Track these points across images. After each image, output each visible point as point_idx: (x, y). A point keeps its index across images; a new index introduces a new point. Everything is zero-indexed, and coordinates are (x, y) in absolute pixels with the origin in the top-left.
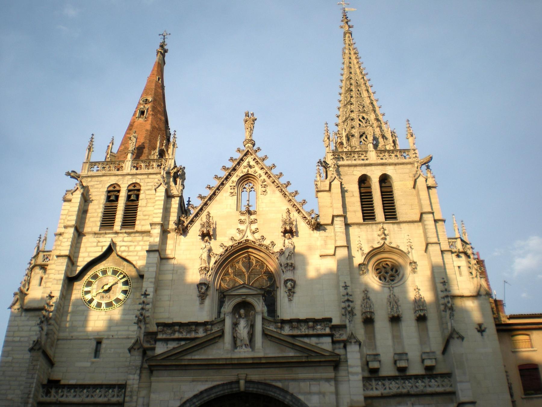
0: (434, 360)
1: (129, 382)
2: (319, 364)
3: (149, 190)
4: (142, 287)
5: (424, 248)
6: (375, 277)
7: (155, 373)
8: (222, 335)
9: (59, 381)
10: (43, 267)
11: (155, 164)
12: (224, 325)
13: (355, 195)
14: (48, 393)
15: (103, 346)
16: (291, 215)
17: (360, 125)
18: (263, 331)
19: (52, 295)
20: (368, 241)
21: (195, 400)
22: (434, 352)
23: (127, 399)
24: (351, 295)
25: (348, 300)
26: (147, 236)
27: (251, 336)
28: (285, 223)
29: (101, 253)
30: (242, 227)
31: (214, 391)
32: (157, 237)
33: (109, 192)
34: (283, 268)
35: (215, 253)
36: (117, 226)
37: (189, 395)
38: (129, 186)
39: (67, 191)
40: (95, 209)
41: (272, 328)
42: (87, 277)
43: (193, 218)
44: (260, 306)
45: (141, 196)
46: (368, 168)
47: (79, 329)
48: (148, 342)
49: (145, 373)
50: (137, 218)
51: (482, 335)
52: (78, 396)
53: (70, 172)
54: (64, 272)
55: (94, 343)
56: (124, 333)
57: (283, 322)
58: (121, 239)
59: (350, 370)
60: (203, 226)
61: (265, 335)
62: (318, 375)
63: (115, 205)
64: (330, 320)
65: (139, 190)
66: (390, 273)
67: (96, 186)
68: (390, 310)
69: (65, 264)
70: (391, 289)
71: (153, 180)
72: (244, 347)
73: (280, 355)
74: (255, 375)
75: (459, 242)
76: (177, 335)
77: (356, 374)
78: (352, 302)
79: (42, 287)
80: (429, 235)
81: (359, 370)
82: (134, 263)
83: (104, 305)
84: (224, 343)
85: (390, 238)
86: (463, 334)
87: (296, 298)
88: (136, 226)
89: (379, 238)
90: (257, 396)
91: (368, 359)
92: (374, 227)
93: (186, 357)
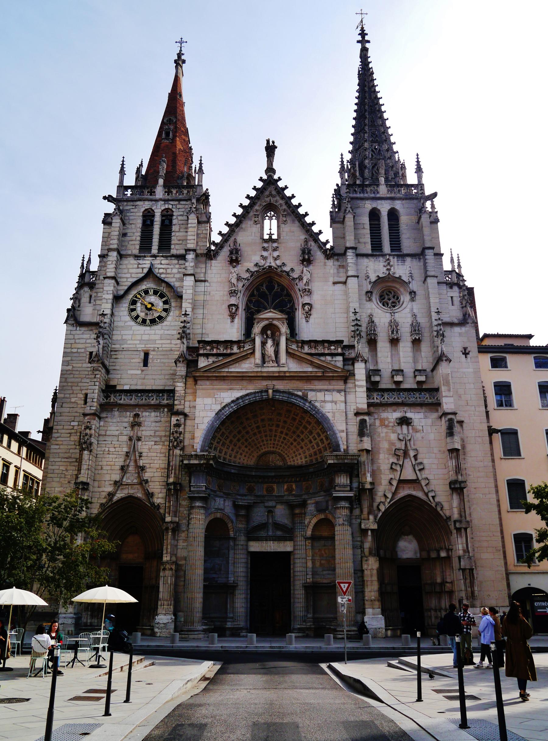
0: (424, 377)
1: (177, 389)
2: (332, 378)
3: (181, 215)
4: (181, 307)
5: (423, 279)
6: (379, 303)
7: (199, 382)
8: (253, 353)
9: (115, 386)
10: (92, 286)
11: (185, 192)
12: (255, 343)
13: (366, 227)
14: (107, 397)
15: (150, 357)
17: (372, 155)
18: (287, 350)
19: (105, 313)
20: (375, 271)
21: (232, 405)
22: (425, 370)
23: (176, 402)
24: (359, 320)
25: (357, 325)
26: (182, 260)
27: (277, 353)
28: (303, 252)
29: (143, 275)
31: (247, 398)
32: (192, 262)
33: (144, 216)
34: (301, 293)
35: (243, 277)
36: (155, 250)
37: (228, 400)
38: (162, 211)
39: (105, 214)
40: (134, 233)
41: (294, 347)
42: (130, 297)
44: (284, 329)
45: (174, 222)
46: (379, 202)
47: (129, 342)
48: (190, 355)
49: (190, 381)
50: (173, 242)
51: (466, 357)
52: (133, 399)
53: (107, 196)
54: (111, 292)
55: (142, 355)
56: (167, 346)
57: (304, 342)
58: (158, 262)
59: (357, 383)
60: (231, 252)
61: (289, 354)
62: (331, 387)
63: (150, 229)
64: (341, 342)
65: (172, 215)
66: (392, 300)
67: (132, 210)
68: (390, 333)
69: (112, 285)
70: (393, 314)
71: (184, 206)
72: (271, 362)
73: (301, 370)
74: (280, 385)
75: (454, 275)
76: (215, 351)
77: (361, 386)
78: (360, 326)
79: (92, 304)
80: (429, 268)
81: (364, 383)
82: (172, 284)
83: (148, 322)
84: (255, 359)
85: (394, 268)
86: (450, 357)
87: (312, 320)
88: (172, 250)
89: (385, 269)
90: (282, 402)
91: (371, 374)
92: (381, 258)
93: (223, 370)
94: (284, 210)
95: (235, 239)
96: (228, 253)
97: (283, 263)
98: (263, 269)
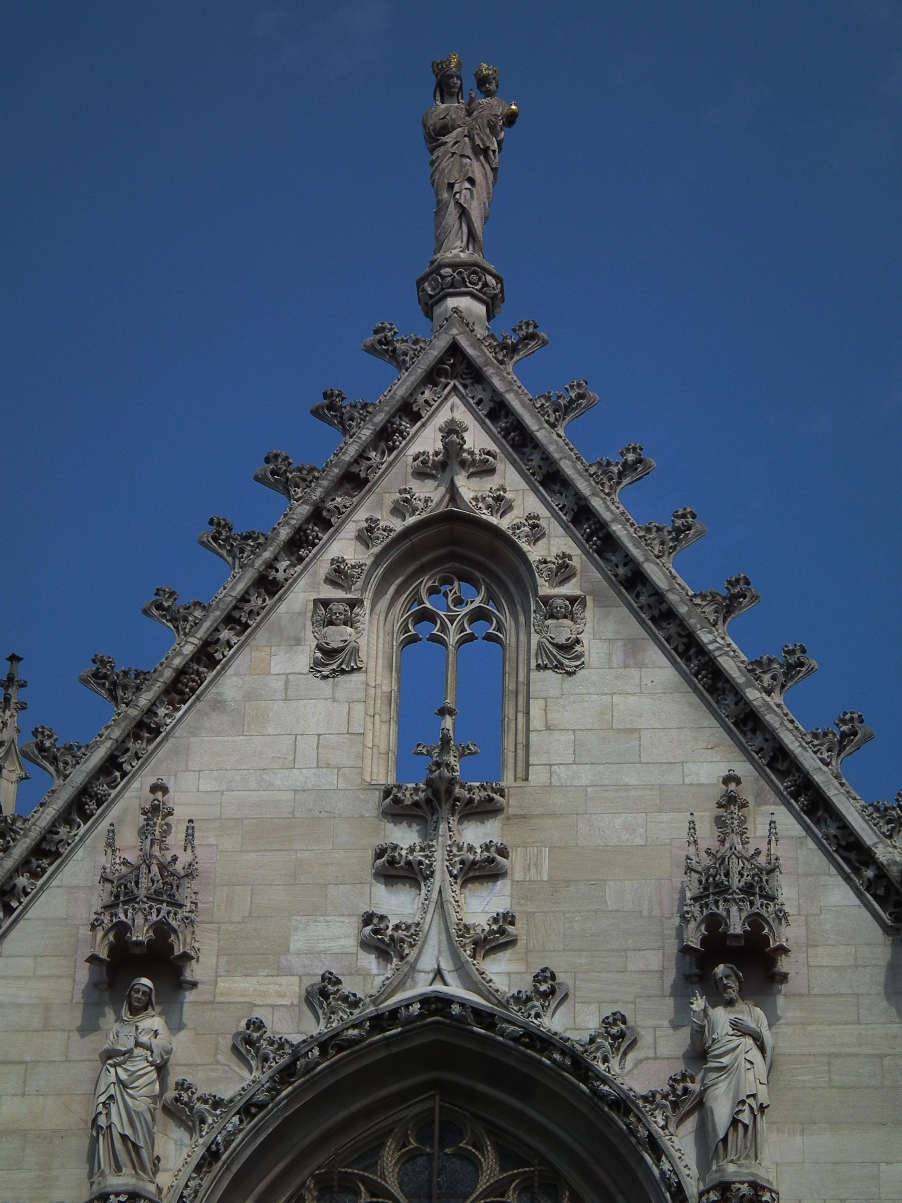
16: (758, 829)
28: (712, 887)
30: (398, 905)
43: (52, 830)
60: (122, 891)
94: (563, 571)
95: (159, 788)
96: (99, 897)
97: (545, 975)
98: (379, 1022)
